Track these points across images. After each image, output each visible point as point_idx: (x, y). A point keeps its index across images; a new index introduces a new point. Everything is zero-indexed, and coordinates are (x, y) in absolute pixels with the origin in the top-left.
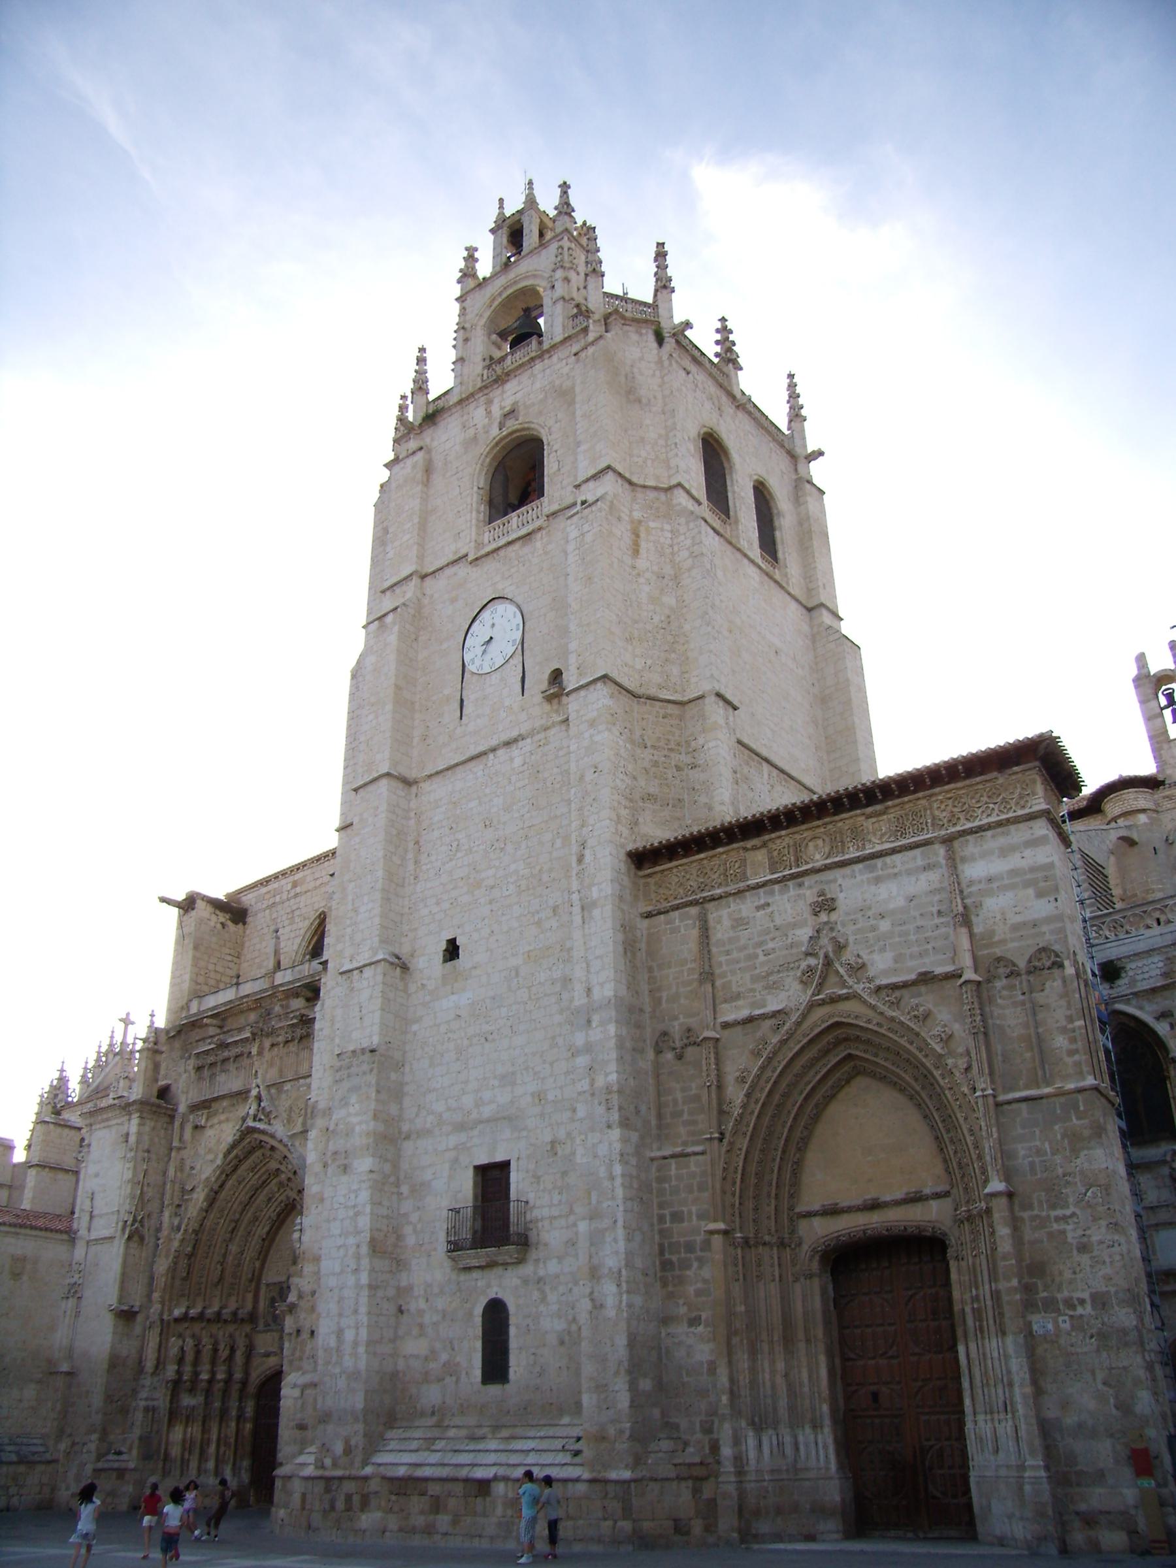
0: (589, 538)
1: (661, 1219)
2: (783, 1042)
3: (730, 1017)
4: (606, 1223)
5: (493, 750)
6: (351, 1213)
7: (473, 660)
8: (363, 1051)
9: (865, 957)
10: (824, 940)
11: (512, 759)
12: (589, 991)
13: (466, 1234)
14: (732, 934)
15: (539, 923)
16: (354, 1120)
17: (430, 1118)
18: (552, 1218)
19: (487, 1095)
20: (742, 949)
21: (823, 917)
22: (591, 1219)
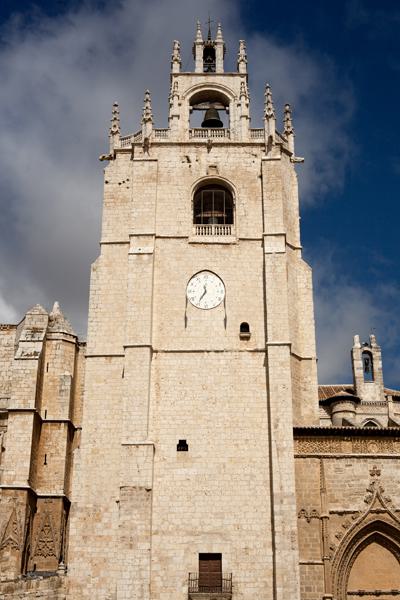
0: (279, 270)
1: (301, 589)
2: (357, 524)
3: (334, 510)
4: (292, 590)
5: (208, 352)
6: (137, 569)
7: (193, 299)
8: (141, 488)
9: (391, 498)
10: (376, 487)
11: (219, 360)
12: (281, 487)
13: (195, 584)
14: (334, 473)
15: (237, 445)
16: (135, 522)
17: (171, 526)
18: (245, 583)
19: (207, 521)
20: (339, 481)
21: (376, 477)
22: (284, 587)
